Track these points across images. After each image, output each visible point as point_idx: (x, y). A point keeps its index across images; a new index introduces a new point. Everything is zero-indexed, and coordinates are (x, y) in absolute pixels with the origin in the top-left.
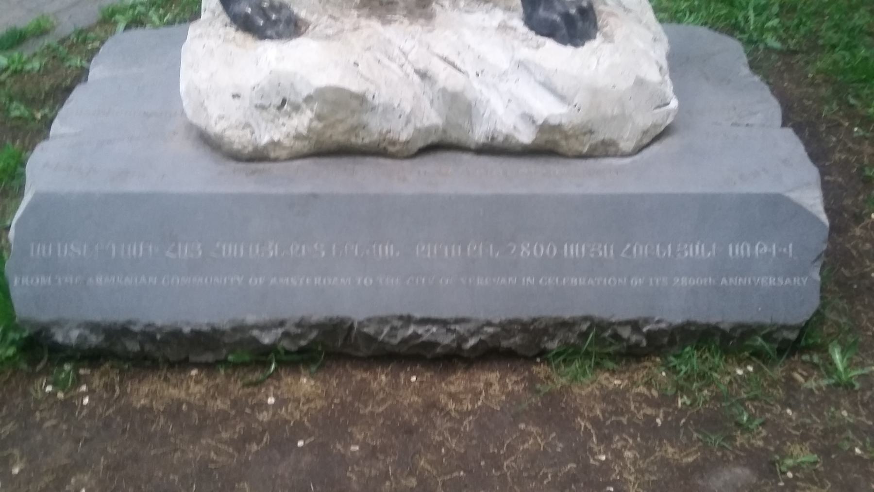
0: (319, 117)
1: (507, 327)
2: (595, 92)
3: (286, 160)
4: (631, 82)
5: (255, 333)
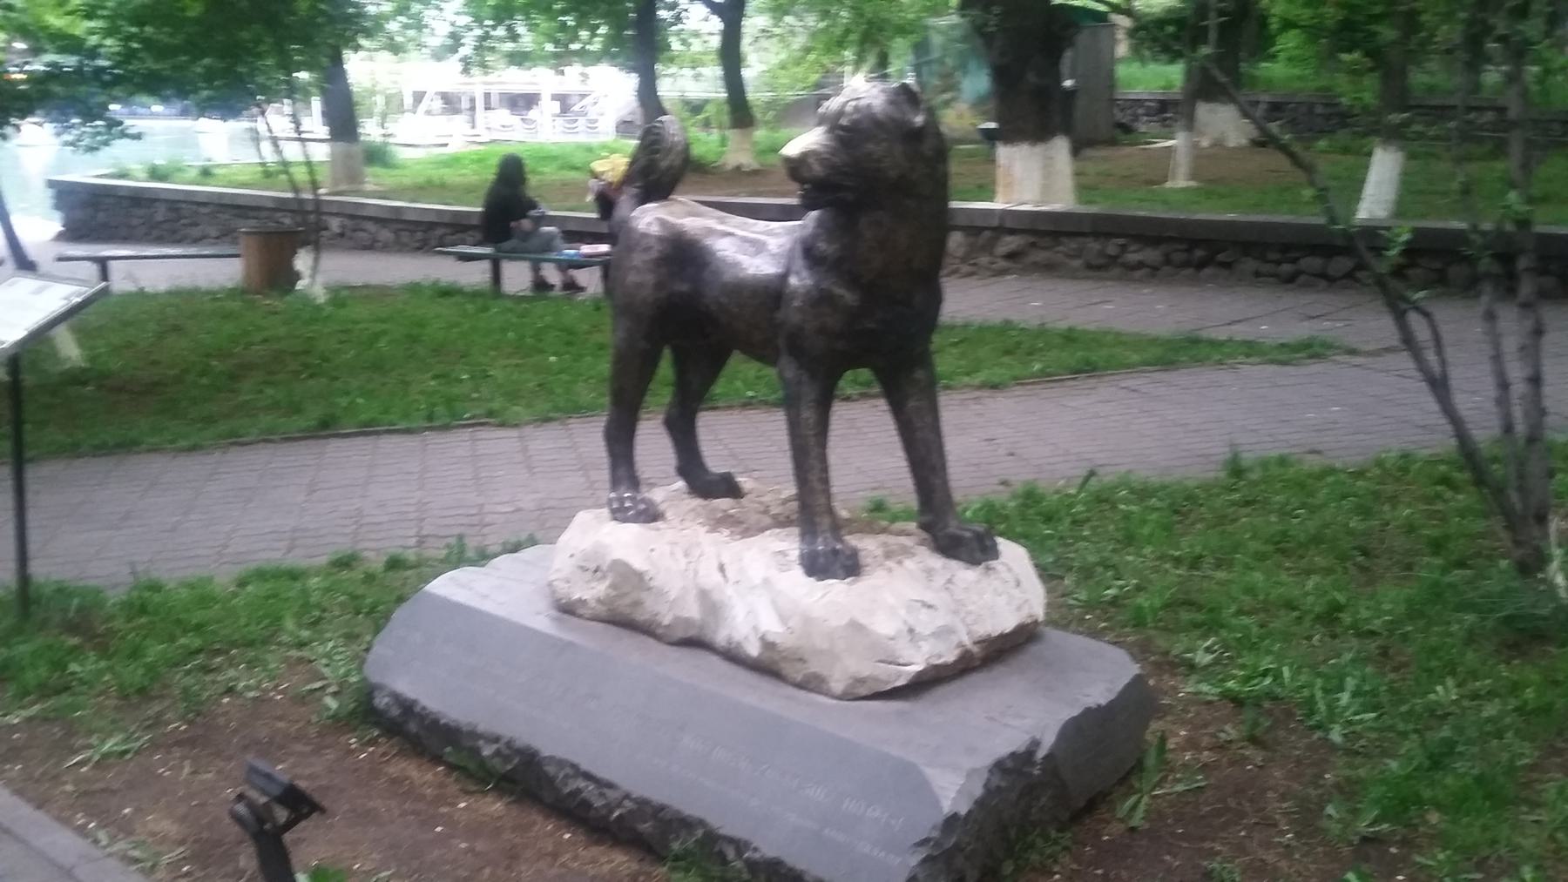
0: (613, 586)
1: (646, 808)
2: (808, 620)
3: (588, 619)
4: (844, 622)
5: (481, 742)
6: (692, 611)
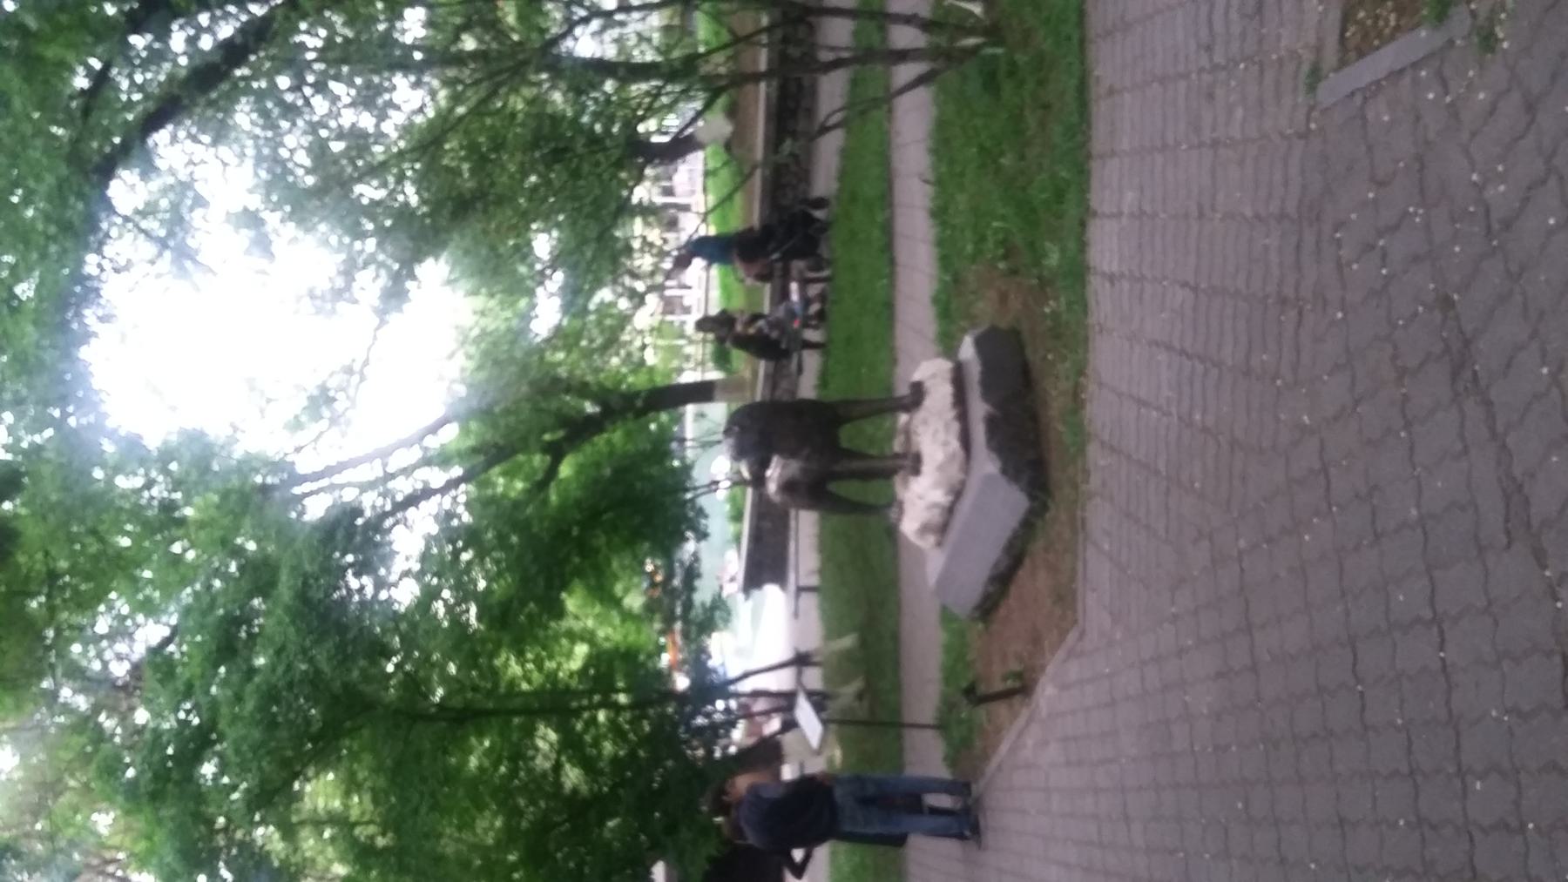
6: (936, 512)
